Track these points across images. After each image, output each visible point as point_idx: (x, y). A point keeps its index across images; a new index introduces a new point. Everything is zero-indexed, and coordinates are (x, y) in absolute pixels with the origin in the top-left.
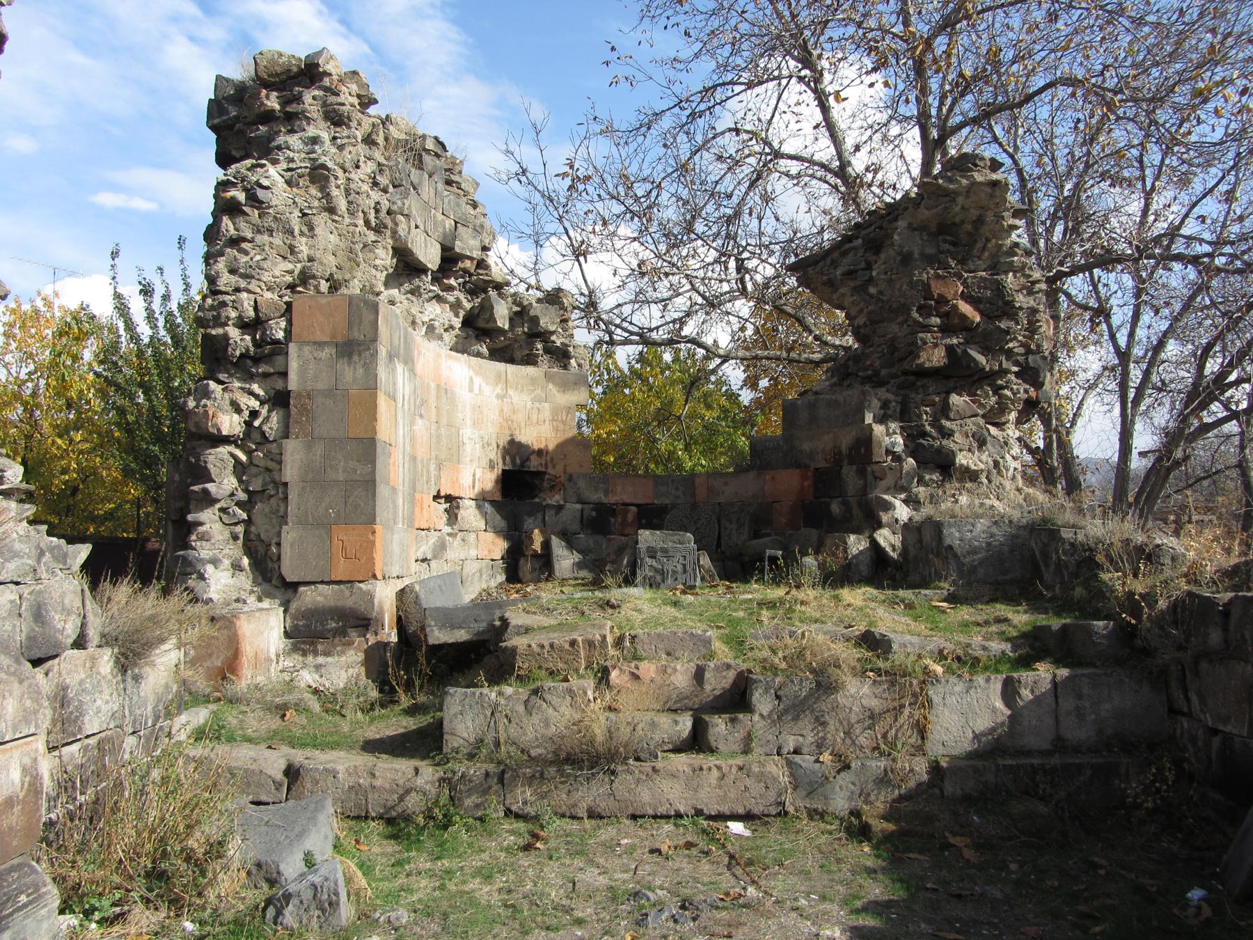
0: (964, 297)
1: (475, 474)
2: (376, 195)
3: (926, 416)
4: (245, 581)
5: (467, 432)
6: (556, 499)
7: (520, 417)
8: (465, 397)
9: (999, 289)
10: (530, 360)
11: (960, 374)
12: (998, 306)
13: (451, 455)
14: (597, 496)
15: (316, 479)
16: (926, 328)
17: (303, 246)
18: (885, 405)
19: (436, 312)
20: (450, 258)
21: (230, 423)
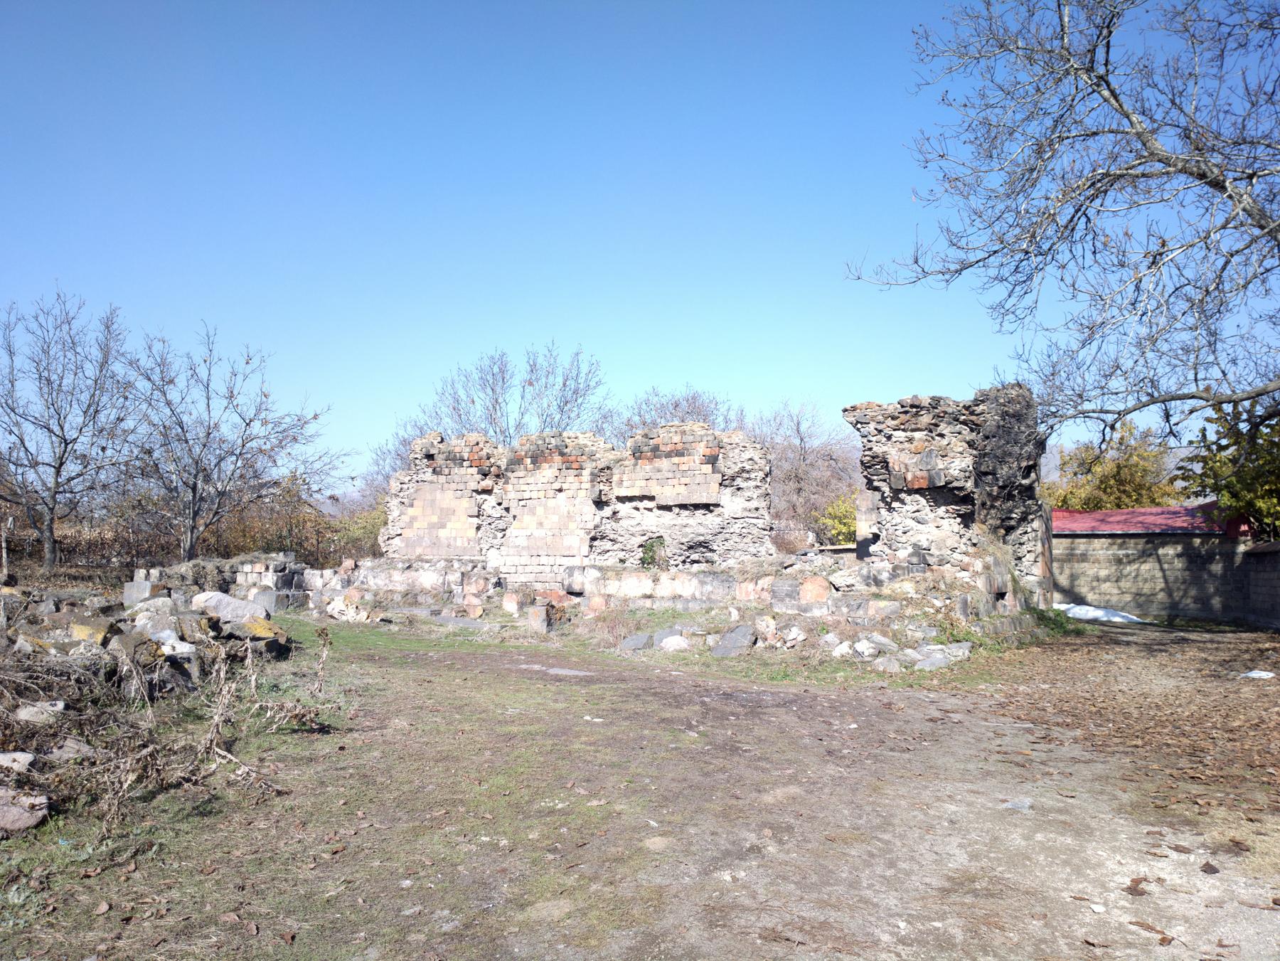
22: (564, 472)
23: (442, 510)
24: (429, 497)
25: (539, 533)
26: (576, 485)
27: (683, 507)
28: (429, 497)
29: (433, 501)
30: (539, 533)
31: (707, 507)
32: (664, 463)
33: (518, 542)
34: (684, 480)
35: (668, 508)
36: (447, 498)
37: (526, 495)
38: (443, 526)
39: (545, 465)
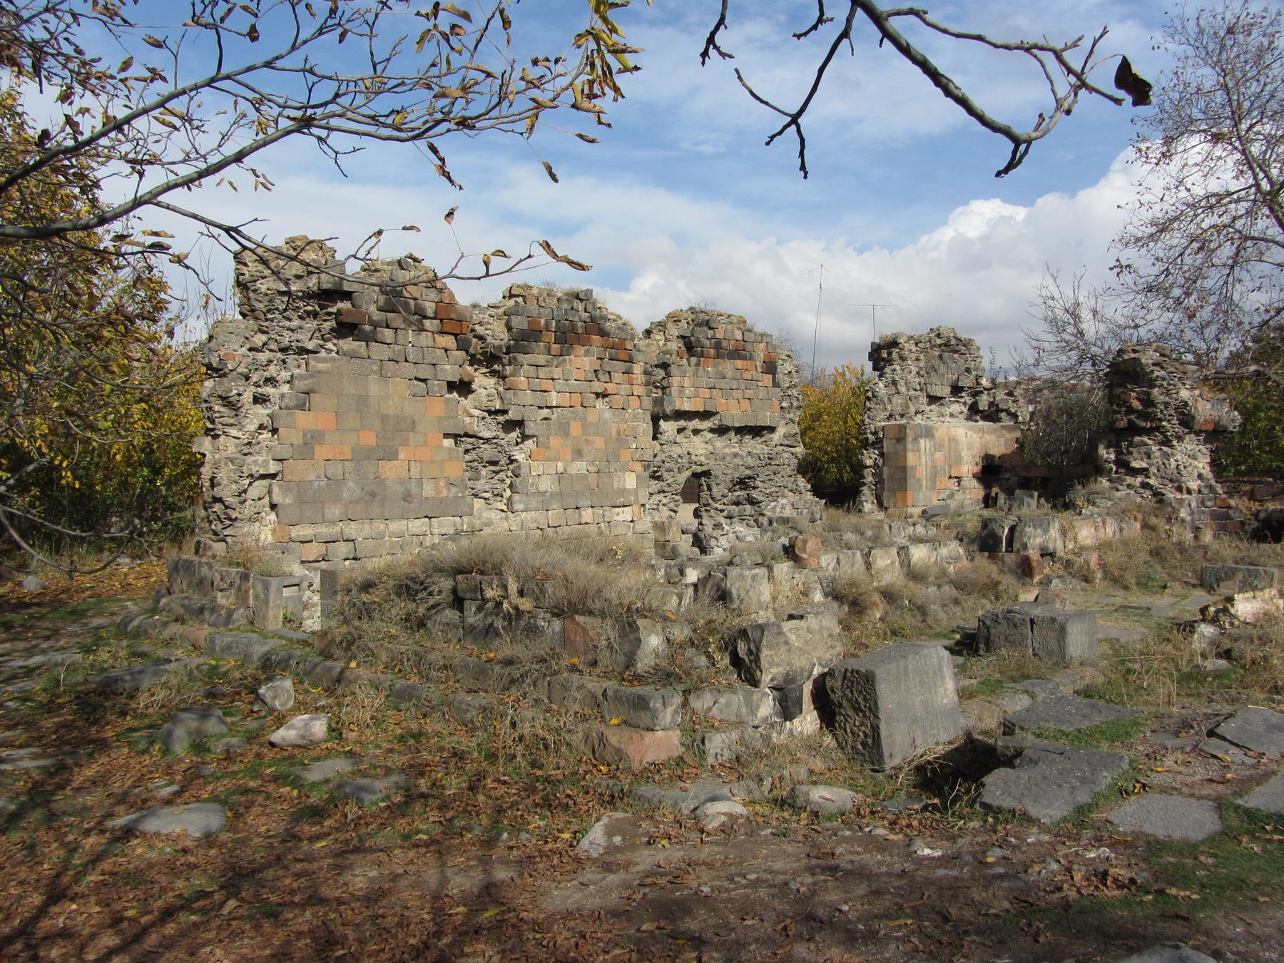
0: (1137, 399)
1: (969, 468)
2: (917, 380)
3: (1124, 444)
4: (875, 506)
5: (964, 453)
6: (1008, 475)
7: (991, 445)
8: (963, 439)
9: (1148, 394)
10: (999, 420)
11: (1133, 430)
12: (1148, 402)
13: (959, 461)
14: (1023, 474)
15: (891, 478)
16: (1119, 412)
17: (889, 407)
18: (1110, 441)
19: (956, 408)
20: (956, 390)
21: (869, 462)
22: (609, 365)
23: (384, 418)
24: (350, 388)
25: (579, 467)
26: (625, 389)
27: (741, 431)
28: (350, 388)
29: (362, 400)
30: (579, 467)
31: (756, 431)
32: (729, 367)
33: (546, 485)
34: (749, 393)
35: (721, 431)
36: (394, 395)
37: (554, 399)
38: (391, 456)
39: (581, 350)
